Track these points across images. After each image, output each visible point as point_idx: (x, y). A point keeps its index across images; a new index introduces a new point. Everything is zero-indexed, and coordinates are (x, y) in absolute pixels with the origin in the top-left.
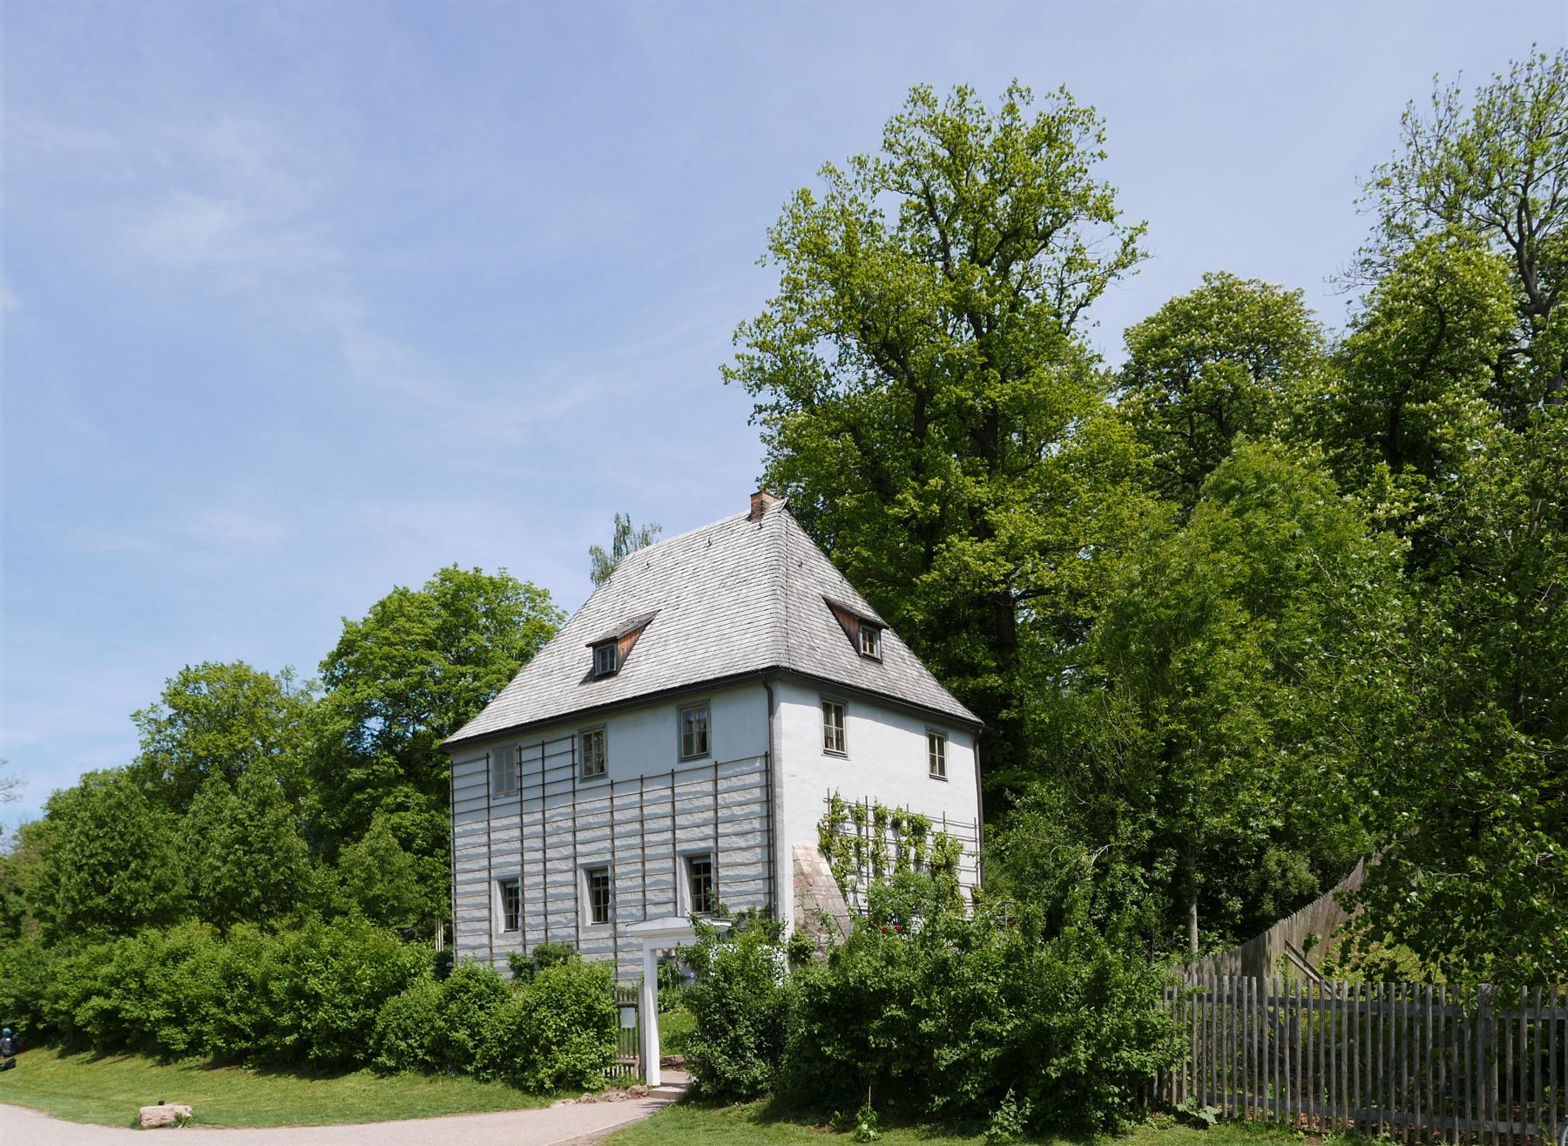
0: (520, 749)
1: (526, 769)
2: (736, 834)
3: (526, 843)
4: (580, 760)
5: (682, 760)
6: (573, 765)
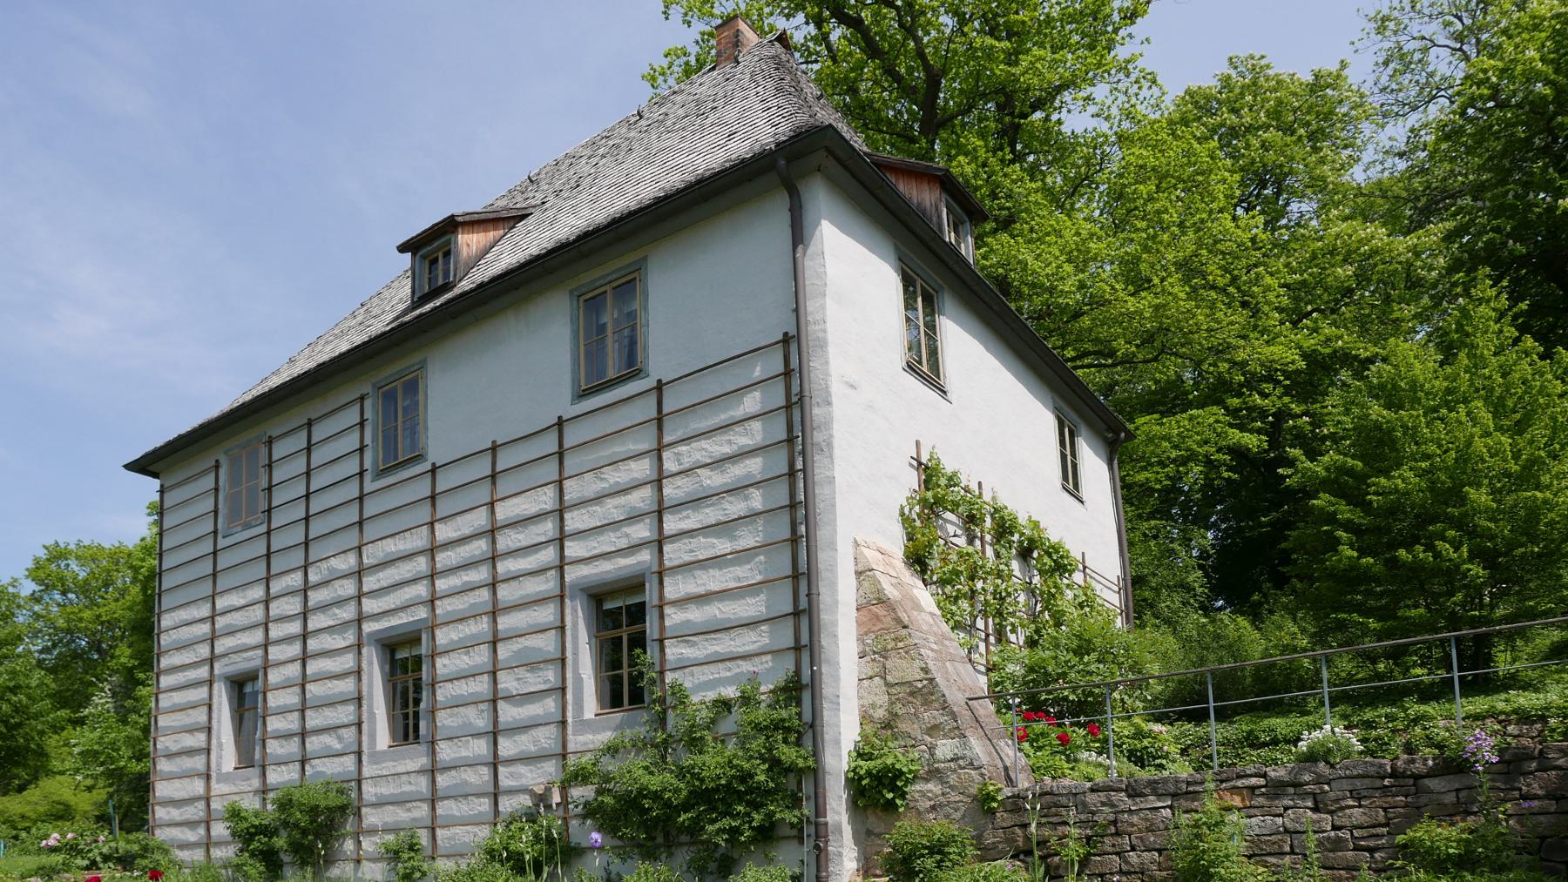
0: (270, 442)
1: (278, 476)
2: (705, 530)
4: (375, 439)
5: (582, 394)
6: (361, 449)
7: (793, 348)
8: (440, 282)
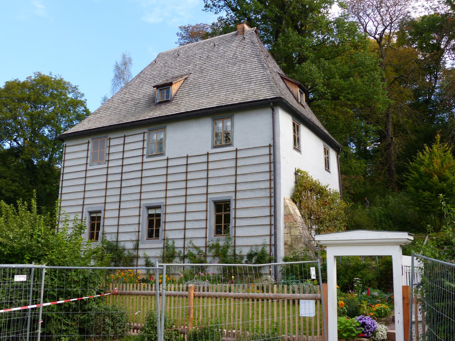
0: (110, 139)
1: (112, 150)
3: (238, 170)
6: (143, 148)
7: (272, 148)
8: (165, 100)
